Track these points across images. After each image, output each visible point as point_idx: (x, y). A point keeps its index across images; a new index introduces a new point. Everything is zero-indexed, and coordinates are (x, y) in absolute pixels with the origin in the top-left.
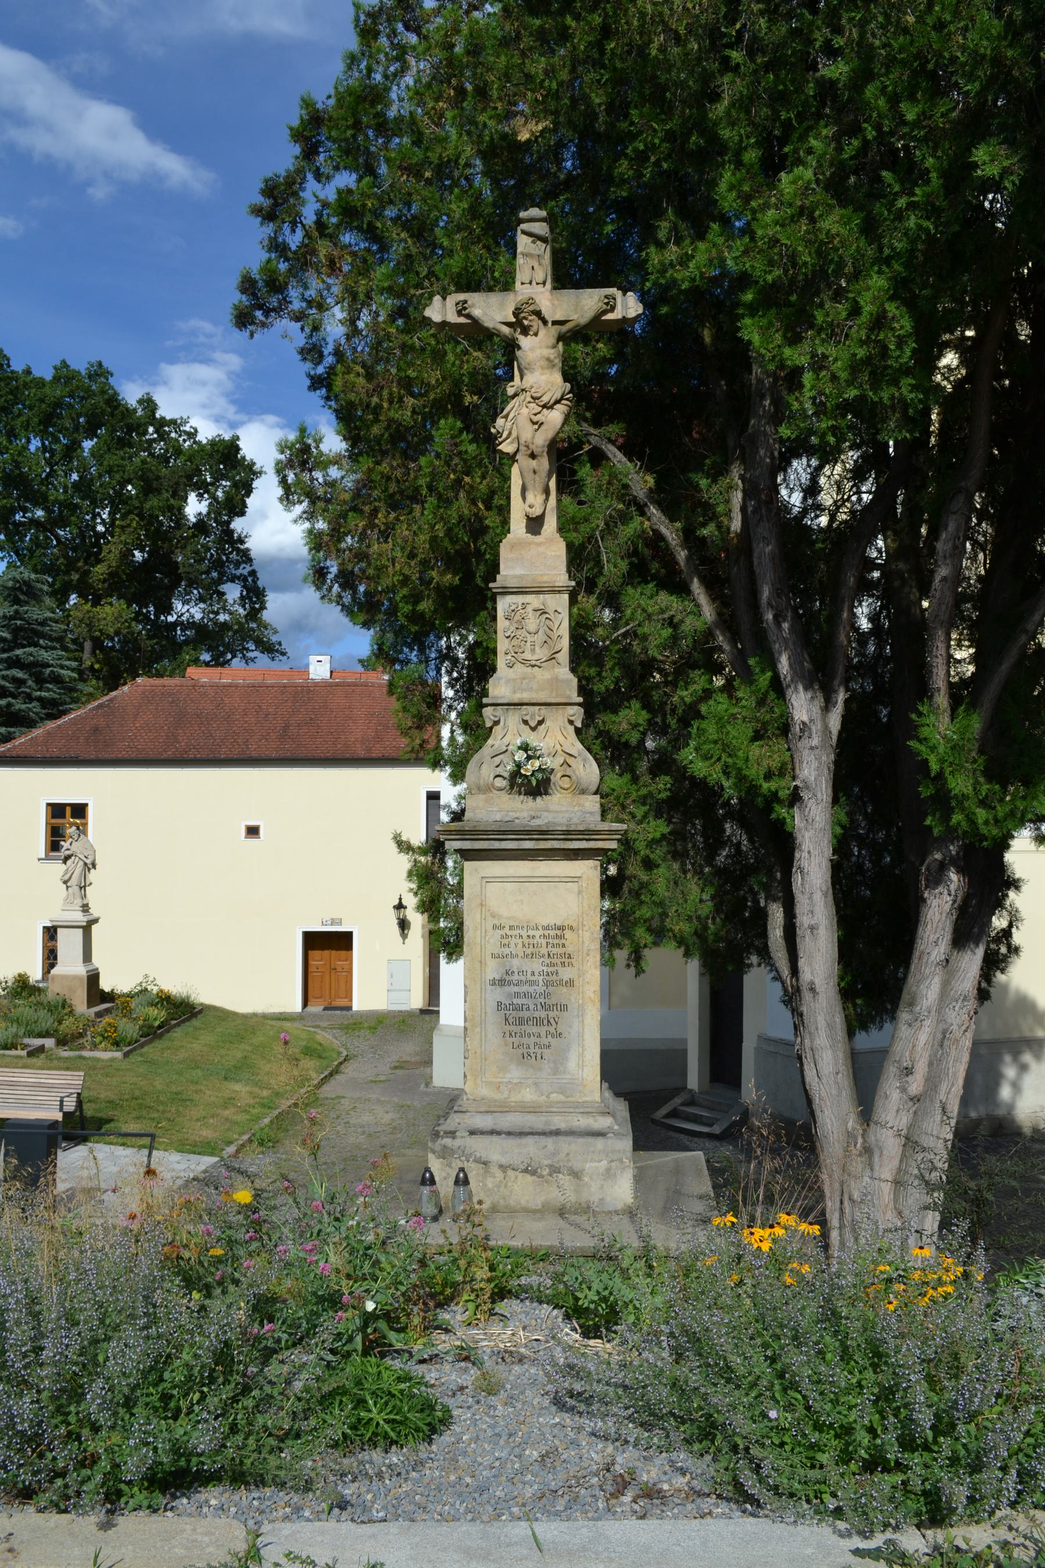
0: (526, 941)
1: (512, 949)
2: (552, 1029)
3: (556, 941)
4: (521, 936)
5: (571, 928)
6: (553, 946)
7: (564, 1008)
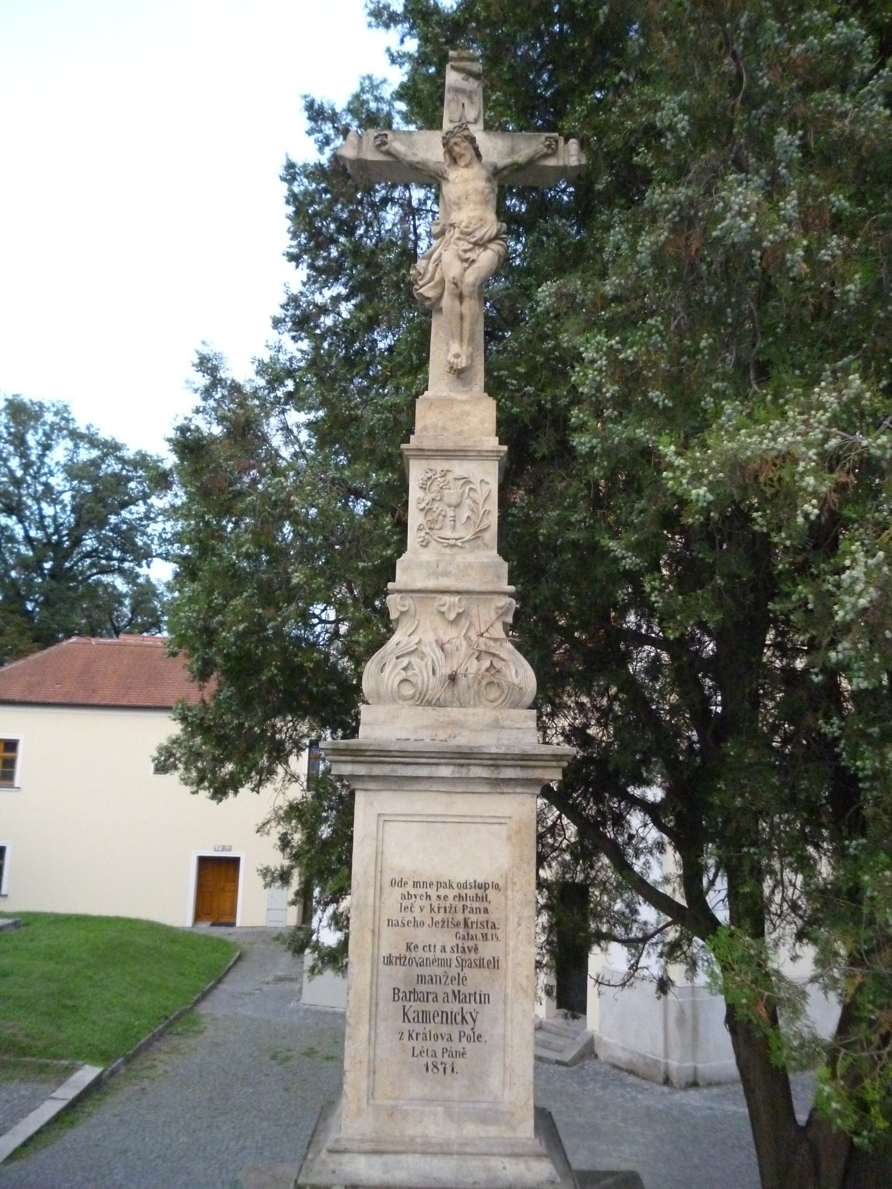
0: (435, 904)
2: (467, 1029)
3: (475, 905)
4: (428, 897)
5: (497, 887)
7: (484, 999)
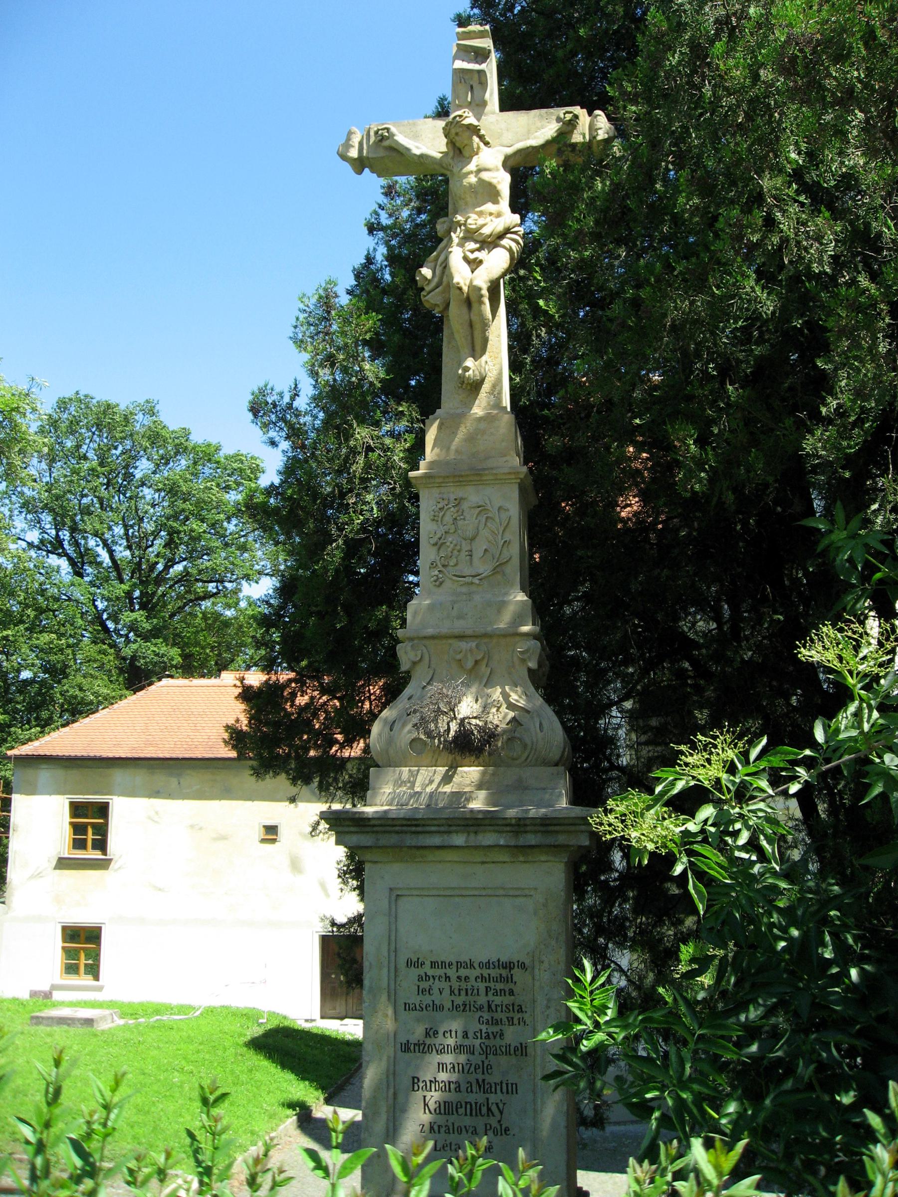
0: (455, 985)
1: (436, 997)
2: (493, 1122)
3: (500, 986)
4: (448, 978)
5: (523, 966)
6: (496, 994)
7: (512, 1089)
